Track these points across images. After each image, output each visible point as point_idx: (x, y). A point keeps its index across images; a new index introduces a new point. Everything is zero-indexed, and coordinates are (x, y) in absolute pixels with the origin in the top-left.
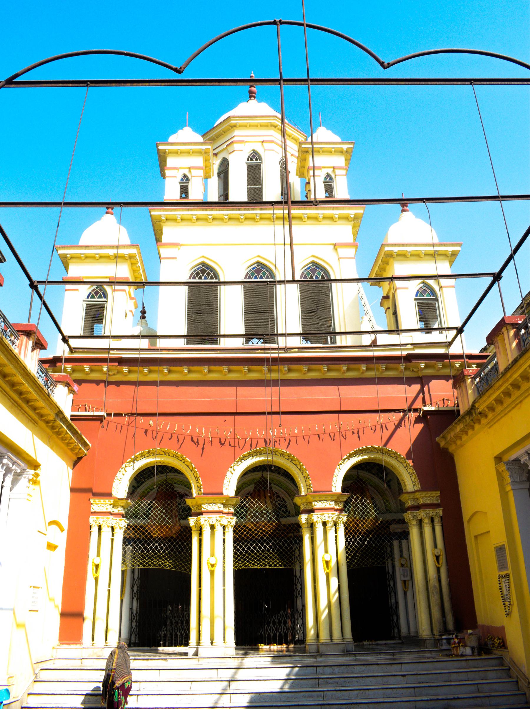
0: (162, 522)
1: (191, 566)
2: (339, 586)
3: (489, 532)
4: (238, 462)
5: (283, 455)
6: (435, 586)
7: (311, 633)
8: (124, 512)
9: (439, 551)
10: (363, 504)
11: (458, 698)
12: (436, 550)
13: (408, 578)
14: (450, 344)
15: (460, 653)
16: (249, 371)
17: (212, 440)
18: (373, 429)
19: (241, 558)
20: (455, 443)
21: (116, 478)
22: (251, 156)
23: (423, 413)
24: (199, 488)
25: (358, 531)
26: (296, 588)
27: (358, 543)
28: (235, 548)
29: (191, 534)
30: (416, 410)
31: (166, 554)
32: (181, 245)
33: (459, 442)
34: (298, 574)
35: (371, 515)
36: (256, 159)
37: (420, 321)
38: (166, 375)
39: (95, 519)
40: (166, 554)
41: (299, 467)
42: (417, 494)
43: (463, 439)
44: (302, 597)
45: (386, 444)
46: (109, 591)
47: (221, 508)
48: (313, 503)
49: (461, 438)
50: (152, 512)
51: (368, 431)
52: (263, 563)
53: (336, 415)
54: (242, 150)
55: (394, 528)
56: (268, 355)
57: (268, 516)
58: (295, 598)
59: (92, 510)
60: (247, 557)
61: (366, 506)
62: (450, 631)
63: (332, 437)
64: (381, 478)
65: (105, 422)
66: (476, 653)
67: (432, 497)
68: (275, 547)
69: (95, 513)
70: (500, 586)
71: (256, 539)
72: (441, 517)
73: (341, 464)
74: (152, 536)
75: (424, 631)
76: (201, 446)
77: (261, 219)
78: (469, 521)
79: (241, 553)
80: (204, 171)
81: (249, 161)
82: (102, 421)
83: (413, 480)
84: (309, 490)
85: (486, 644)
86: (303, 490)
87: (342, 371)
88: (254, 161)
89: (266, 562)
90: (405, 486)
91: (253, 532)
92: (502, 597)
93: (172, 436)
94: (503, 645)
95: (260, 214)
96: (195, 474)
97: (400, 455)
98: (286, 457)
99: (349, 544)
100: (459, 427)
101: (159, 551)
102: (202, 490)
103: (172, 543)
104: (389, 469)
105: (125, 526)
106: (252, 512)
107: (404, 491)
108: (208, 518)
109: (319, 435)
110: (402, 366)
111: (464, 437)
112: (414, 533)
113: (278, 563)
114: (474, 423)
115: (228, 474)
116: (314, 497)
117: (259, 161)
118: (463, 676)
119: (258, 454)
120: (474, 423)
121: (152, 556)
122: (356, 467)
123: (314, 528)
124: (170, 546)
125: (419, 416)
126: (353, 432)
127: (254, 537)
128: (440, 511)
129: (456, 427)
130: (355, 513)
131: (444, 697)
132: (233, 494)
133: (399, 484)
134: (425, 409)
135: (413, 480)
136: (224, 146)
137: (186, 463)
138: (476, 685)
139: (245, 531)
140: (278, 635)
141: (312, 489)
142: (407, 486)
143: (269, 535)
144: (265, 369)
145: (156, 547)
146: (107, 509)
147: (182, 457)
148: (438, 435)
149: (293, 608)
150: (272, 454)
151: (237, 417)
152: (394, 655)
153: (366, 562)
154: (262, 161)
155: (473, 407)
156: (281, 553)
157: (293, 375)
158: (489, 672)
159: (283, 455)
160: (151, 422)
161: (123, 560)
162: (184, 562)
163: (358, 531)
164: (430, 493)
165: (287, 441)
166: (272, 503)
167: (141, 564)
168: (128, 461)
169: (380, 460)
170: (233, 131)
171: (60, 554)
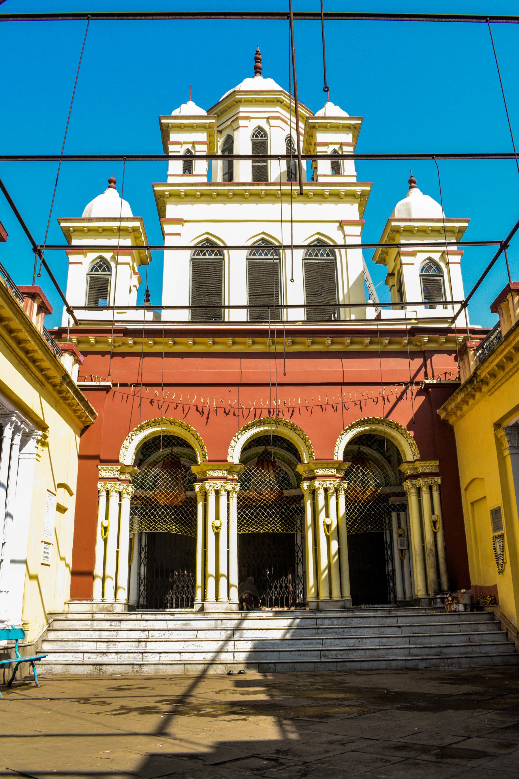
1: (196, 531)
2: (339, 549)
3: (485, 497)
4: (242, 431)
5: (286, 424)
6: (431, 549)
7: (311, 592)
8: (131, 479)
9: (436, 517)
10: (364, 474)
11: (450, 646)
12: (433, 516)
13: (405, 547)
14: (454, 319)
15: (453, 609)
17: (216, 410)
18: (376, 400)
19: (245, 523)
20: (455, 414)
21: (122, 446)
22: (256, 133)
23: (425, 386)
24: (204, 456)
26: (297, 556)
27: (358, 510)
28: (239, 513)
30: (417, 383)
31: (173, 519)
33: (459, 413)
34: (299, 543)
36: (262, 136)
38: (171, 347)
39: (103, 484)
40: (173, 519)
41: (302, 437)
42: (417, 463)
44: (303, 564)
45: (387, 416)
46: (117, 552)
48: (315, 471)
49: (461, 409)
51: (370, 403)
52: (266, 528)
57: (271, 484)
58: (296, 564)
59: (100, 476)
60: (251, 522)
61: (366, 476)
62: (444, 591)
63: (335, 409)
65: (111, 393)
66: (469, 610)
67: (431, 466)
68: (278, 513)
69: (103, 479)
70: (494, 547)
71: (260, 506)
72: (439, 485)
73: (343, 434)
74: (158, 503)
75: (420, 591)
76: (205, 416)
77: (266, 195)
78: (466, 489)
79: (245, 518)
80: (208, 147)
81: (255, 138)
83: (413, 450)
84: (311, 458)
85: (478, 603)
86: (305, 458)
87: (346, 344)
88: (260, 138)
89: (269, 527)
90: (405, 456)
92: (496, 556)
93: (177, 406)
95: (265, 190)
96: (200, 442)
97: (401, 426)
98: (289, 427)
99: (349, 511)
101: (165, 516)
102: (207, 457)
104: (390, 441)
105: (132, 492)
107: (404, 461)
108: (213, 483)
109: (321, 406)
110: (405, 340)
112: (413, 500)
113: (280, 528)
114: (475, 391)
115: (233, 442)
116: (316, 464)
117: (264, 138)
118: (455, 628)
119: (262, 423)
120: (475, 391)
121: (159, 521)
123: (316, 494)
124: (176, 512)
125: (421, 388)
126: (355, 403)
129: (457, 398)
130: (355, 482)
131: (437, 645)
133: (399, 454)
134: (427, 382)
135: (413, 450)
136: (229, 122)
137: (191, 432)
138: (468, 636)
140: (279, 598)
141: (314, 457)
142: (407, 456)
143: (272, 502)
144: (269, 341)
145: (163, 513)
146: (114, 475)
147: (187, 426)
149: (295, 574)
150: (276, 424)
151: (241, 388)
152: (390, 612)
153: (365, 527)
154: (267, 138)
156: (283, 518)
157: (297, 348)
158: (480, 625)
159: (286, 425)
160: (157, 392)
161: (130, 524)
162: (189, 527)
165: (291, 412)
166: (274, 471)
168: (134, 429)
169: (381, 431)
170: (238, 107)
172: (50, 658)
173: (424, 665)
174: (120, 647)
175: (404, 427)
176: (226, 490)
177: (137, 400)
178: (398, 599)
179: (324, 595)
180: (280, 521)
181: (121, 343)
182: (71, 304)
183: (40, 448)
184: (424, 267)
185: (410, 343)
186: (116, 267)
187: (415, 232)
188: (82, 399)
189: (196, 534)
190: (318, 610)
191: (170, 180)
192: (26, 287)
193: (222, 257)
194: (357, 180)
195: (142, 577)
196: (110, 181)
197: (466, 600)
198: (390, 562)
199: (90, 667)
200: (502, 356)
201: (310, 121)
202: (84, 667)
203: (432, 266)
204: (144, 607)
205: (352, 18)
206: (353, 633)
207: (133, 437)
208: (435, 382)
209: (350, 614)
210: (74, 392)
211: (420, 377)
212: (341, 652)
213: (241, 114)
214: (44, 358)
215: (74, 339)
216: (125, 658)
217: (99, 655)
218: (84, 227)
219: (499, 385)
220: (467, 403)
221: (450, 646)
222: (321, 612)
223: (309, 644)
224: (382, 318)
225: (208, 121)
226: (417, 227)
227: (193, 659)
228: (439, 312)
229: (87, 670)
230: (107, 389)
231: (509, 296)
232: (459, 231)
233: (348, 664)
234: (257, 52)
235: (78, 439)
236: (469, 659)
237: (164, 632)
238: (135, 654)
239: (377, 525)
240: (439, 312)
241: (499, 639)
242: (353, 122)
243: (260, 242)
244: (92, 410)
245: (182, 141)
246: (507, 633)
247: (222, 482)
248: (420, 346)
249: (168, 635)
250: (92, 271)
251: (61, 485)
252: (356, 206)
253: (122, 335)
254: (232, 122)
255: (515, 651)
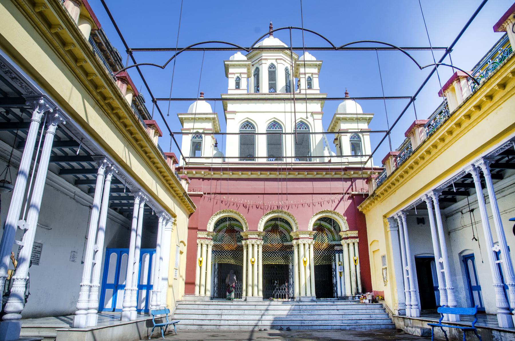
0: (229, 243)
3: (379, 249)
5: (285, 213)
11: (361, 319)
13: (342, 271)
16: (270, 174)
18: (328, 202)
20: (366, 209)
24: (247, 228)
25: (319, 248)
27: (319, 254)
29: (243, 248)
30: (348, 194)
31: (231, 257)
32: (237, 112)
34: (291, 268)
35: (326, 241)
36: (273, 68)
37: (352, 151)
39: (199, 241)
40: (231, 257)
42: (347, 232)
43: (370, 207)
47: (257, 237)
48: (299, 235)
49: (368, 207)
50: (224, 238)
51: (325, 202)
53: (311, 195)
54: (266, 63)
55: (336, 248)
56: (280, 167)
57: (278, 241)
59: (198, 237)
64: (331, 225)
66: (371, 302)
69: (199, 238)
72: (358, 243)
74: (224, 249)
75: (348, 293)
76: (247, 209)
78: (370, 245)
79: (265, 257)
81: (270, 69)
82: (201, 196)
85: (376, 299)
88: (272, 69)
90: (342, 228)
91: (271, 248)
94: (383, 299)
100: (368, 202)
103: (234, 252)
106: (271, 239)
107: (341, 231)
111: (370, 206)
115: (260, 221)
116: (299, 232)
117: (274, 69)
118: (364, 311)
122: (320, 219)
124: (233, 254)
125: (350, 196)
127: (271, 250)
128: (358, 240)
130: (318, 240)
132: (262, 231)
133: (339, 228)
134: (353, 193)
136: (257, 61)
139: (267, 247)
144: (278, 173)
145: (227, 254)
147: (239, 213)
148: (358, 205)
151: (264, 195)
155: (374, 193)
156: (284, 257)
163: (319, 248)
164: (353, 231)
165: (288, 207)
166: (280, 235)
167: (220, 261)
171: (184, 255)
172: (182, 322)
173: (349, 328)
174: (209, 317)
175: (342, 214)
176: (257, 244)
177: (215, 201)
178: (338, 296)
179: (303, 294)
180: (283, 258)
181: (207, 174)
182: (184, 156)
183: (173, 226)
184: (352, 137)
185: (344, 174)
186: (205, 137)
187: (348, 120)
188: (191, 202)
189: (243, 265)
190: (300, 301)
191: (230, 92)
192: (168, 153)
193: (254, 130)
194: (320, 92)
195: (216, 283)
196: (201, 94)
197: (371, 298)
198: (335, 278)
199: (197, 326)
200: (386, 186)
201: (297, 62)
202: (194, 326)
203: (356, 136)
204: (216, 298)
205: (317, 49)
206: (316, 312)
207: (213, 219)
208: (357, 193)
209: (315, 303)
210: (187, 199)
211: (350, 191)
212: (311, 321)
213: (263, 57)
214: (177, 186)
215: (186, 171)
216: (212, 322)
217: (200, 321)
218: (190, 117)
219: (385, 198)
220: (371, 205)
221: (361, 319)
222: (301, 302)
223: (296, 317)
224: (332, 162)
225: (247, 63)
226: (349, 117)
227: (243, 323)
228: (358, 159)
229: (195, 327)
230: (201, 196)
231: (390, 158)
232: (369, 119)
233: (314, 326)
234: (271, 24)
235: (188, 219)
236: (370, 326)
237: (229, 311)
238: (217, 321)
239: (328, 261)
240: (358, 159)
241: (384, 316)
242: (318, 63)
243: (273, 122)
244: (194, 206)
245: (235, 72)
246: (388, 314)
247: (255, 240)
248: (350, 176)
249: (231, 312)
250: (193, 138)
251: (182, 242)
252: (319, 105)
253: (208, 170)
254: (259, 61)
255: (392, 323)
